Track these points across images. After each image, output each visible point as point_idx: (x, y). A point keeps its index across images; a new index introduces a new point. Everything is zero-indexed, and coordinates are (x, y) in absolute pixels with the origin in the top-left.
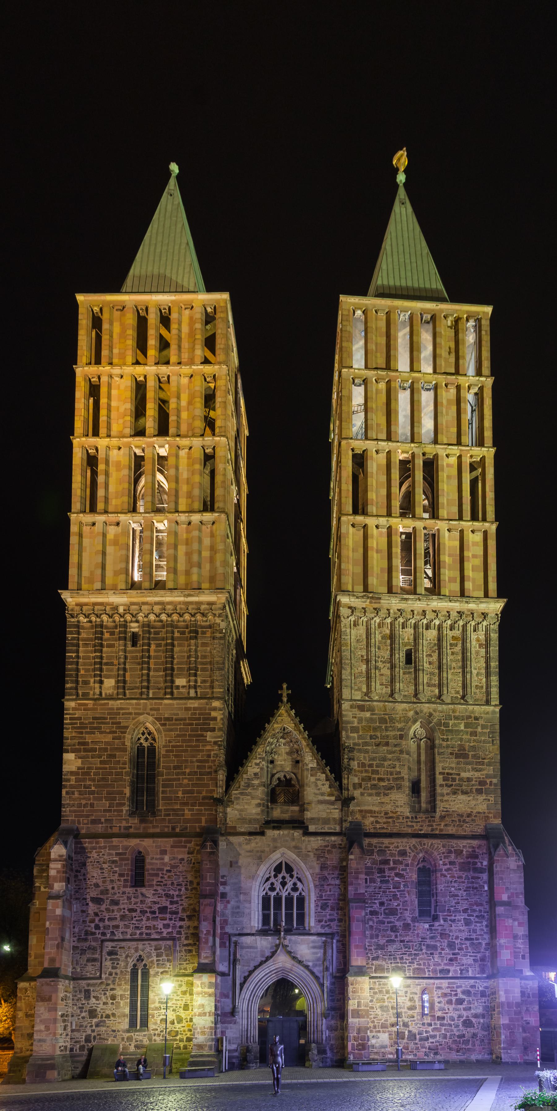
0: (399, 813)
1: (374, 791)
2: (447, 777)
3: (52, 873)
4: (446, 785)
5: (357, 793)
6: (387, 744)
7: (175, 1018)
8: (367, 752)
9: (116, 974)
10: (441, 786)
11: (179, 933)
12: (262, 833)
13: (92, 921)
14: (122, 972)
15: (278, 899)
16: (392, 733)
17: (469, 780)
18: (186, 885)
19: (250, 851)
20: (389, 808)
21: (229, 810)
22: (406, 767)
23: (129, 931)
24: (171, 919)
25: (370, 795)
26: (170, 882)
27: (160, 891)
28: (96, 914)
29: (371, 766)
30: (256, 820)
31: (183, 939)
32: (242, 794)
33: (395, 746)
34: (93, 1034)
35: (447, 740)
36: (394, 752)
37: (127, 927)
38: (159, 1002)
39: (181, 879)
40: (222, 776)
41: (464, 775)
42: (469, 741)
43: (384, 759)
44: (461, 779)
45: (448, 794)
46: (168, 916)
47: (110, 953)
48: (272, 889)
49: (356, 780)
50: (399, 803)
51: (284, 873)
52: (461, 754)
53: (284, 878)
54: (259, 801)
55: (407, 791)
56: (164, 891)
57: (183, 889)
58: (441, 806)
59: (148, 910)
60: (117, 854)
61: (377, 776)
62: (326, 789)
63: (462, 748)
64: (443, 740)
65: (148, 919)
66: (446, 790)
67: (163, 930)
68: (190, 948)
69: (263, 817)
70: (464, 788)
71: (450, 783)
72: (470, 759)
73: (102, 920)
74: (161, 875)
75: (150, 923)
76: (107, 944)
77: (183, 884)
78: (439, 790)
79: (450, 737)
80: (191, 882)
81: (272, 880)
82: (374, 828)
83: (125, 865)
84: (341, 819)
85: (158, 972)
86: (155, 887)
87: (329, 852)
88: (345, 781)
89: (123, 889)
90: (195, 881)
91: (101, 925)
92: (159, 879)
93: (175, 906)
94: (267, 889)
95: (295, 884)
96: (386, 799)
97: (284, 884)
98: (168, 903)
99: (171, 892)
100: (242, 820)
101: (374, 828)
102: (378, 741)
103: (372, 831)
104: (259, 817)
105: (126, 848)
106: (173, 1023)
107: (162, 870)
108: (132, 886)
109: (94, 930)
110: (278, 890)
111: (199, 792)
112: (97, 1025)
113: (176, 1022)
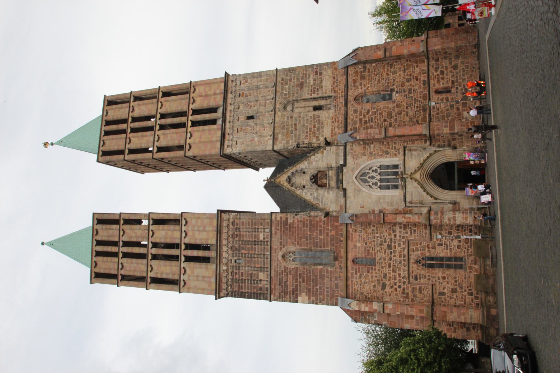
1: (321, 130)
2: (313, 92)
3: (367, 309)
5: (322, 139)
6: (295, 125)
8: (299, 135)
9: (429, 276)
10: (318, 94)
11: (403, 237)
12: (345, 190)
13: (396, 290)
14: (428, 272)
15: (381, 180)
17: (314, 80)
20: (330, 121)
21: (331, 210)
22: (308, 113)
23: (402, 267)
24: (395, 242)
25: (323, 131)
26: (373, 243)
27: (378, 249)
28: (392, 287)
29: (307, 132)
30: (337, 194)
31: (407, 235)
32: (322, 202)
33: (296, 120)
34: (468, 291)
35: (293, 93)
37: (399, 269)
38: (447, 249)
40: (312, 213)
41: (312, 83)
42: (294, 82)
43: (303, 125)
44: (314, 84)
45: (322, 90)
46: (393, 244)
47: (416, 279)
48: (376, 184)
49: (314, 140)
50: (327, 115)
51: (367, 178)
52: (301, 85)
53: (369, 178)
54: (326, 192)
55: (320, 112)
57: (377, 235)
59: (389, 256)
60: (356, 273)
61: (313, 129)
62: (319, 156)
63: (297, 86)
64: (293, 95)
65: (395, 256)
66: (320, 91)
67: (402, 247)
68: (413, 231)
69: (335, 191)
70: (319, 82)
71: (316, 90)
72: (304, 81)
73: (395, 284)
75: (397, 254)
76: (411, 281)
78: (320, 95)
80: (373, 230)
81: (371, 184)
83: (362, 269)
84: (336, 146)
85: (428, 251)
86: (376, 251)
87: (355, 152)
88: (315, 145)
89: (377, 271)
90: (372, 228)
91: (398, 284)
92: (371, 249)
95: (373, 171)
96: (325, 123)
97: (373, 178)
99: (379, 242)
100: (337, 201)
103: (343, 129)
105: (352, 268)
106: (460, 241)
107: (365, 247)
108: (375, 266)
109: (402, 289)
110: (377, 181)
111: (321, 226)
112: (462, 288)
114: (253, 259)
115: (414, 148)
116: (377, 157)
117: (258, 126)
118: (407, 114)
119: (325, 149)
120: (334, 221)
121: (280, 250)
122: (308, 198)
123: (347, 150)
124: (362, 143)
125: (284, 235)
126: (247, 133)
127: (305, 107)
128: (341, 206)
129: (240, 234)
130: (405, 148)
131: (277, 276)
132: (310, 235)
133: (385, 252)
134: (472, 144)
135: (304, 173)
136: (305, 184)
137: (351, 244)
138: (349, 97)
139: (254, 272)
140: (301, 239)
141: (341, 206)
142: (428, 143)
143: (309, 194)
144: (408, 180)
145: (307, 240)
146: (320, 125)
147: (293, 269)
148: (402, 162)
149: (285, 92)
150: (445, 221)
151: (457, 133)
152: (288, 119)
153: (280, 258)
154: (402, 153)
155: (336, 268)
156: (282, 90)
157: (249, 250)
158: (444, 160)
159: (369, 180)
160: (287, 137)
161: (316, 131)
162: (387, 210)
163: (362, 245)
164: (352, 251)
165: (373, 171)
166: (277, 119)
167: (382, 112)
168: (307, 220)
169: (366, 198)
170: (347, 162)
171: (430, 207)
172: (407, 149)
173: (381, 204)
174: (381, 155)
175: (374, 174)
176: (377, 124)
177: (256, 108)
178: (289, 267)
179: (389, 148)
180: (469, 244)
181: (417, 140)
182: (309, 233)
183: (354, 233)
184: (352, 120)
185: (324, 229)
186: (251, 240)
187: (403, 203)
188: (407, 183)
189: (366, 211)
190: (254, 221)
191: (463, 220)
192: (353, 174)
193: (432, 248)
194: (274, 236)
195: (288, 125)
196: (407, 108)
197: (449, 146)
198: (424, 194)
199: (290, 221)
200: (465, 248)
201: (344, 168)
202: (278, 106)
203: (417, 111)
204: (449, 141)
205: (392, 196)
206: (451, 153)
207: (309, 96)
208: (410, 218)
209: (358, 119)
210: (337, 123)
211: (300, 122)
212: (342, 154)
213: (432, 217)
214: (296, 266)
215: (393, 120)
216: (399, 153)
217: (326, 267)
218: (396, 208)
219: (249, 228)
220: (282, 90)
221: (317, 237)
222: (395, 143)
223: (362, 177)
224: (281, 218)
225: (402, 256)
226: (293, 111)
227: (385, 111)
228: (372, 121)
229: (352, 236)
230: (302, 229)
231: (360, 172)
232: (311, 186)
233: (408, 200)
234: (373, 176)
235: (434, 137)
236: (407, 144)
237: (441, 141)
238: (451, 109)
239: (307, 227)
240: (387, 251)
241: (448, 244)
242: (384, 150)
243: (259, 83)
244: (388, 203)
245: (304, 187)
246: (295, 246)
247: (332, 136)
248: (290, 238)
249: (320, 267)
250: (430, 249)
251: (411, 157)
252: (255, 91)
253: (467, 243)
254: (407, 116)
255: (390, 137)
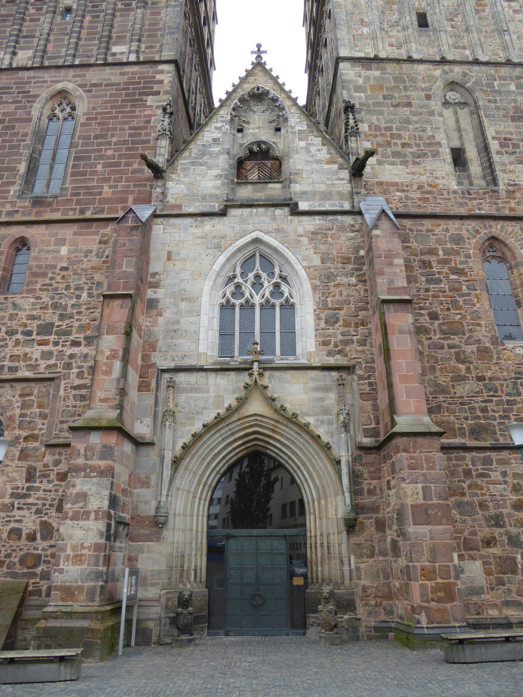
0: (441, 187)
1: (398, 160)
2: (505, 142)
4: (506, 153)
6: (409, 105)
7: (38, 527)
8: (382, 113)
10: (498, 153)
11: (68, 366)
12: (223, 213)
15: (248, 306)
16: (414, 94)
18: (91, 288)
19: (202, 237)
20: (423, 179)
24: (56, 344)
25: (393, 164)
26: (64, 286)
32: (193, 164)
36: (421, 114)
39: (84, 280)
43: (408, 121)
45: (511, 163)
46: (52, 338)
50: (439, 174)
53: (258, 277)
54: (219, 172)
55: (449, 158)
56: (52, 298)
57: (84, 295)
58: (503, 178)
61: (399, 142)
62: (324, 153)
64: (490, 101)
65: (17, 343)
66: (506, 158)
69: (223, 192)
71: (511, 149)
74: (50, 275)
75: (19, 351)
77: (86, 287)
78: (496, 158)
79: (498, 99)
80: (99, 284)
82: (404, 206)
85: (18, 438)
86: (38, 293)
92: (47, 281)
93: (67, 322)
94: (228, 295)
95: (277, 286)
97: (257, 284)
98: (56, 317)
100: (193, 197)
101: (404, 206)
102: (395, 102)
104: (218, 192)
106: (32, 538)
110: (247, 295)
113: (38, 535)
114: (67, 37)
115: (349, 396)
116: (318, 294)
117: (400, 34)
118: (459, 379)
119: (341, 168)
120: (139, 192)
121: (79, 85)
122: (206, 134)
123: (339, 217)
124: (362, 253)
125: (117, 89)
126: (383, 12)
127: (459, 129)
128: (180, 207)
129: (132, 10)
130: (348, 369)
131: (14, 84)
132: (109, 143)
133: (33, 318)
134: (364, 589)
135: (278, 130)
136: (246, 131)
137: (67, 232)
138: (500, 224)
139: (36, 40)
140: (100, 124)
141: (180, 207)
142: (367, 441)
143: (217, 135)
144: (245, 378)
145: (96, 137)
146: (410, 158)
147: (29, 113)
148: (303, 361)
149: (496, 84)
150: (78, 481)
151: (402, 534)
152: (422, 90)
153: (59, 86)
154: (331, 361)
155: (13, 204)
156: (502, 78)
157: (89, 28)
158: (309, 494)
159: (251, 276)
160: (373, 88)
161: (394, 148)
162: (155, 322)
163: (61, 259)
164: (50, 235)
165: (277, 286)
166: (421, 68)
167: (461, 308)
168: (149, 134)
169: (195, 272)
170: (305, 218)
171: (152, 444)
172: (344, 375)
173: (175, 304)
174: (325, 303)
175: (268, 288)
176: (422, 293)
177: (449, 29)
178: (35, 105)
179: (347, 324)
180: (19, 569)
181: (375, 407)
182: (114, 140)
183: (98, 238)
184: (428, 231)
185: (121, 172)
186: (114, 30)
187: (172, 365)
188: (233, 374)
189: (155, 266)
190: (159, 33)
191: (74, 548)
192: (267, 233)
193: (22, 451)
194: (117, 70)
195: (406, 89)
196: (481, 379)
197: (357, 508)
198: (197, 427)
199: (150, 100)
200: (8, 556)
201: (286, 210)
202: (457, 69)
203: (472, 409)
204: (375, 509)
205: (197, 332)
206: (331, 513)
207: (490, 132)
208: (108, 372)
209: (432, 244)
210: (419, 195)
211: (415, 114)
212: (327, 207)
213: (96, 439)
214: (35, 119)
215: (437, 337)
216: (329, 354)
217: (19, 182)
218: (160, 343)
219: (143, 25)
220: (502, 78)
221: (102, 157)
222: (362, 343)
223: (257, 257)
224: (161, 82)
225: (16, 364)
226: (446, 104)
227: (464, 317)
228: (428, 281)
229: (91, 234)
230: (127, 126)
231: (275, 250)
232: (241, 145)
233: (181, 378)
234: (262, 285)
235: (386, 458)
236: (361, 378)
237: (375, 482)
238: (487, 519)
239: (130, 135)
240: (37, 323)
241: (30, 501)
242: (342, 313)
243: (514, 37)
244: (178, 322)
245: (240, 131)
246: (85, 114)
247: (380, 184)
248: (106, 102)
249: (22, 168)
250: (23, 445)
251: (317, 389)
252: (493, 27)
253: (22, 561)
254: (453, 380)
255: (382, 315)
